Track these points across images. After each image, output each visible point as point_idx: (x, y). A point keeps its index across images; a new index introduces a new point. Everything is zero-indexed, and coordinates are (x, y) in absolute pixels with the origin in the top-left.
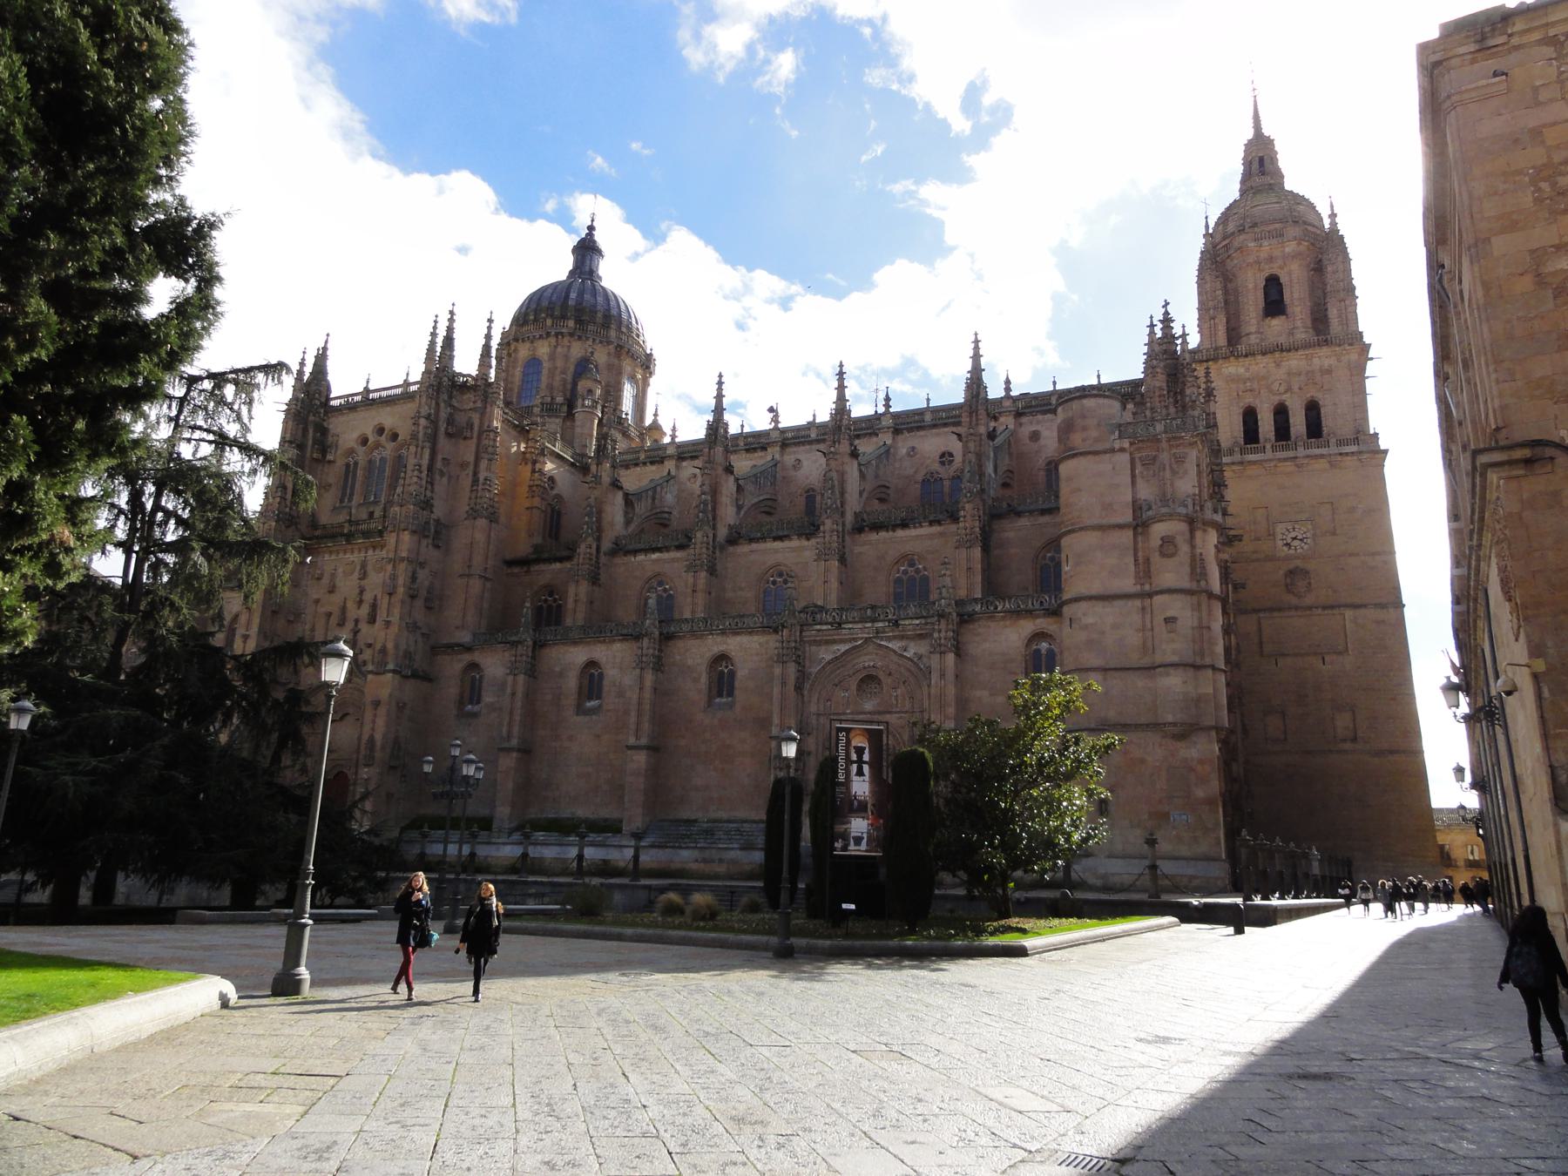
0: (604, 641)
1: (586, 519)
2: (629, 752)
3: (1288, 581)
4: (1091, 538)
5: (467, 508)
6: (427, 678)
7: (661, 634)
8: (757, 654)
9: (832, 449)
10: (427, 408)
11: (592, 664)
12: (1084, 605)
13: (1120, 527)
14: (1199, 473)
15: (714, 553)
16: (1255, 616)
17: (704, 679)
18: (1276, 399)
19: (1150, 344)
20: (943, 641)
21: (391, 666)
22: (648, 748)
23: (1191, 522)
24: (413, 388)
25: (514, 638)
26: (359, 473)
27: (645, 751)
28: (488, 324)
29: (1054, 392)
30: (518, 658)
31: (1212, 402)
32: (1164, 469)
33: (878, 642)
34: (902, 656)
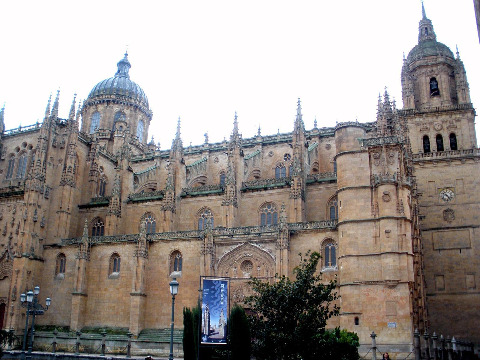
0: (121, 244)
2: (132, 297)
3: (445, 215)
4: (350, 194)
5: (61, 180)
6: (41, 260)
7: (147, 240)
8: (193, 250)
9: (231, 152)
10: (44, 134)
11: (116, 255)
12: (348, 225)
13: (365, 187)
14: (400, 163)
15: (174, 202)
16: (430, 232)
17: (168, 262)
18: (436, 133)
21: (24, 254)
22: (141, 295)
23: (397, 185)
24: (40, 126)
25: (80, 241)
26: (15, 165)
27: (139, 297)
28: (74, 96)
30: (81, 251)
31: (407, 132)
32: (384, 161)
33: (251, 244)
34: (262, 251)
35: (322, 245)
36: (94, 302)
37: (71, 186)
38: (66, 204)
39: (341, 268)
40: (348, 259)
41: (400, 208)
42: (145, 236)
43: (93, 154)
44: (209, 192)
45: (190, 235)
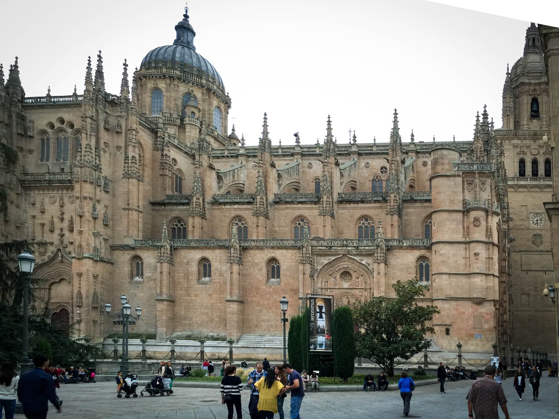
1: (195, 184)
7: (240, 246)
12: (441, 246)
19: (477, 125)
20: (379, 258)
25: (159, 244)
29: (434, 143)
31: (503, 157)
33: (349, 256)
35: (417, 262)
36: (183, 307)
37: (138, 180)
38: (135, 200)
39: (434, 284)
40: (440, 276)
41: (489, 233)
42: (238, 241)
43: (162, 144)
44: (304, 200)
45: (287, 243)
